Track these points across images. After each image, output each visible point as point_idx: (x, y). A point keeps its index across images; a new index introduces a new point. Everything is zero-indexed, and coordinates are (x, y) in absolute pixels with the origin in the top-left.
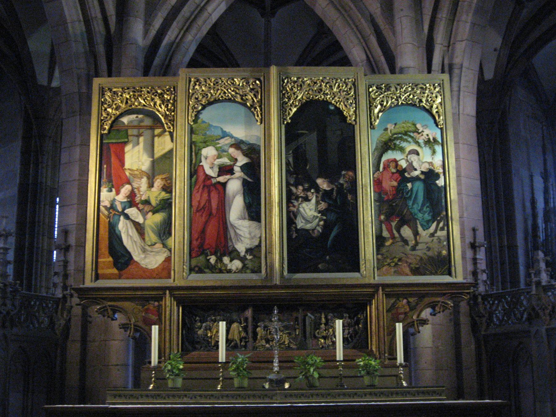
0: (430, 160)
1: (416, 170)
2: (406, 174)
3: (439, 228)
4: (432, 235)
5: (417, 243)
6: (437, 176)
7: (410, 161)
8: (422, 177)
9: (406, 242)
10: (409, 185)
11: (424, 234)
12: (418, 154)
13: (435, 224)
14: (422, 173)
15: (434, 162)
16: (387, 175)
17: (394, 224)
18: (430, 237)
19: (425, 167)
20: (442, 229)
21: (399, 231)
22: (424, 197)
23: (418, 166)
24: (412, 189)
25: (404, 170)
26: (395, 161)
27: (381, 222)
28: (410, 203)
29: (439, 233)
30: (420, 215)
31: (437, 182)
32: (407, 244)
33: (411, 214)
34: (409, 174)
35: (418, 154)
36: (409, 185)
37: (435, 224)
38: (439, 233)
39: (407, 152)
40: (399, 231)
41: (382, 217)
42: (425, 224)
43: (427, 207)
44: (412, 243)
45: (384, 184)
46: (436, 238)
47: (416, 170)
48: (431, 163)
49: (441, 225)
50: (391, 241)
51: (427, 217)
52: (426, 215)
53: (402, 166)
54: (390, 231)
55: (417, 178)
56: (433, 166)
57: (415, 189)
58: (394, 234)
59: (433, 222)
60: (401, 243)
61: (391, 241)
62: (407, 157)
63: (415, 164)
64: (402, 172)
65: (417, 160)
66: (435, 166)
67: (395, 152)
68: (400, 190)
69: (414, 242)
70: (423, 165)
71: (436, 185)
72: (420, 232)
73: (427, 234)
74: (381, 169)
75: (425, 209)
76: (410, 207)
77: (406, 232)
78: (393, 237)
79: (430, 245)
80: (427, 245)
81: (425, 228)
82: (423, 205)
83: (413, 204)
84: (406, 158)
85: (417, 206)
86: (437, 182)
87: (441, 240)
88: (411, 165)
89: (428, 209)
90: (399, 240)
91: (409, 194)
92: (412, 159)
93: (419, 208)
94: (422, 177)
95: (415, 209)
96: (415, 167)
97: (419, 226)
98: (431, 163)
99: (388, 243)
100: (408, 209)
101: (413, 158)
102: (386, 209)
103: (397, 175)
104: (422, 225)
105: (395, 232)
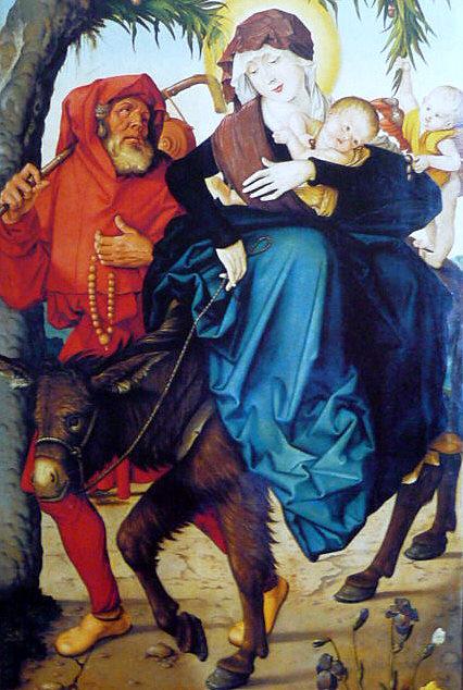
0: (378, 87)
1: (281, 153)
2: (214, 186)
3: (408, 542)
4: (363, 586)
5: (259, 641)
6: (423, 197)
7: (246, 97)
8: (322, 202)
9: (187, 632)
10: (232, 259)
11: (311, 581)
12: (301, 45)
13: (380, 521)
14: (326, 174)
15: (406, 105)
16: (85, 194)
17: (114, 518)
18: (342, 598)
19: (345, 139)
20: (432, 546)
21: (145, 566)
22: (324, 338)
23: (297, 126)
24: (247, 283)
25: (203, 159)
26: (147, 96)
27: (34, 505)
28: (229, 378)
29: (408, 575)
30: (293, 459)
31: (420, 238)
32: (199, 646)
33: (235, 447)
34: (233, 183)
35: (301, 45)
36: (232, 259)
37: (380, 521)
38: (408, 575)
39: (229, 34)
40: (145, 566)
41: (44, 471)
42: (322, 515)
43: (345, 404)
44: (226, 638)
45: (62, 255)
46: (388, 604)
47: (281, 153)
48: (387, 106)
49: (425, 518)
50: (92, 626)
51: (339, 469)
52: (332, 456)
53: (188, 131)
54: (88, 557)
55: (289, 213)
56: (397, 129)
57: (266, 288)
58: (112, 582)
59: (372, 507)
60: (163, 641)
61: (92, 626)
62: (227, 65)
63: (281, 120)
64: (189, 168)
65: (292, 87)
66: (415, 128)
67: (145, 33)
68: (169, 295)
69: (238, 634)
70: (333, 125)
71: (413, 258)
72: (282, 571)
73: (326, 581)
74: (49, 153)
75: (324, 416)
76: (226, 409)
77: (197, 567)
78: (107, 601)
79: (342, 649)
80: (328, 649)
81: (322, 540)
82: (314, 396)
83: (247, 387)
84: (219, 73)
85: (277, 397)
86: (420, 238)
87: (412, 614)
88: (249, 119)
89: (346, 417)
90: (150, 620)
91: (229, 318)
92: (262, 84)
93: (287, 415)
94: (322, 202)
95: (260, 417)
96: (279, 138)
97: (281, 531)
98: (383, 111)
99: (71, 640)
100: (216, 416)
101: (266, 70)
102: (71, 419)
103: (158, 189)
104: (297, 523)
105: (121, 568)
